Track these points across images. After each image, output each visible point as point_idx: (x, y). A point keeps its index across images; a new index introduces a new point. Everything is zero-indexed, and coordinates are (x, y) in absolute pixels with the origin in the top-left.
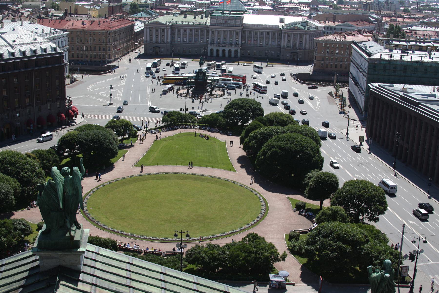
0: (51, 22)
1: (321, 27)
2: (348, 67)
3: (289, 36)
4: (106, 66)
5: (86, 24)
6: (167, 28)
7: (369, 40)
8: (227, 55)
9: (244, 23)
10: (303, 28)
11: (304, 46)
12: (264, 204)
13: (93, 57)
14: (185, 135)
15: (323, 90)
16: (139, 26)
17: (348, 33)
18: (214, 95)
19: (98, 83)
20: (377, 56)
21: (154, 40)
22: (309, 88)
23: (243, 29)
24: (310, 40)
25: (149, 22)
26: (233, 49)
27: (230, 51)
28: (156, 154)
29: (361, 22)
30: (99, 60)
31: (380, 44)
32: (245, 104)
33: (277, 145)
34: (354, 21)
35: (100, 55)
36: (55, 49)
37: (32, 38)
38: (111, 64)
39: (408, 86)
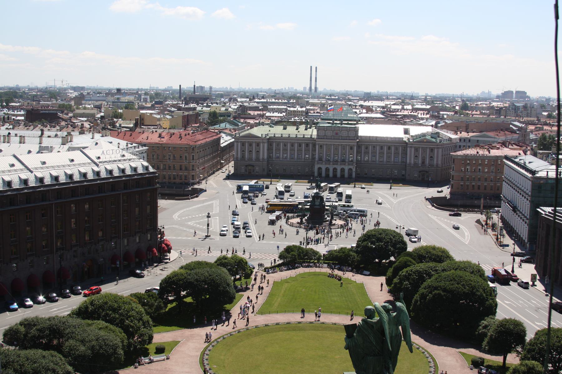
0: (120, 134)
1: (456, 139)
2: (500, 189)
3: (416, 150)
4: (190, 189)
5: (164, 138)
6: (263, 142)
7: (520, 154)
8: (339, 174)
9: (359, 135)
10: (434, 140)
11: (435, 163)
12: (431, 360)
13: (172, 178)
14: (309, 276)
15: (468, 219)
16: (225, 140)
17: (491, 146)
18: (334, 224)
19: (185, 210)
20: (542, 174)
21: (247, 157)
22: (450, 215)
23: (358, 142)
24: (442, 156)
25: (241, 135)
26: (346, 168)
27: (343, 170)
28: (279, 299)
29: (501, 132)
30: (181, 181)
31: (542, 159)
32: (383, 236)
33: (440, 286)
34: (493, 130)
35: (181, 176)
36: (147, 168)
37: (119, 155)
38: (196, 186)
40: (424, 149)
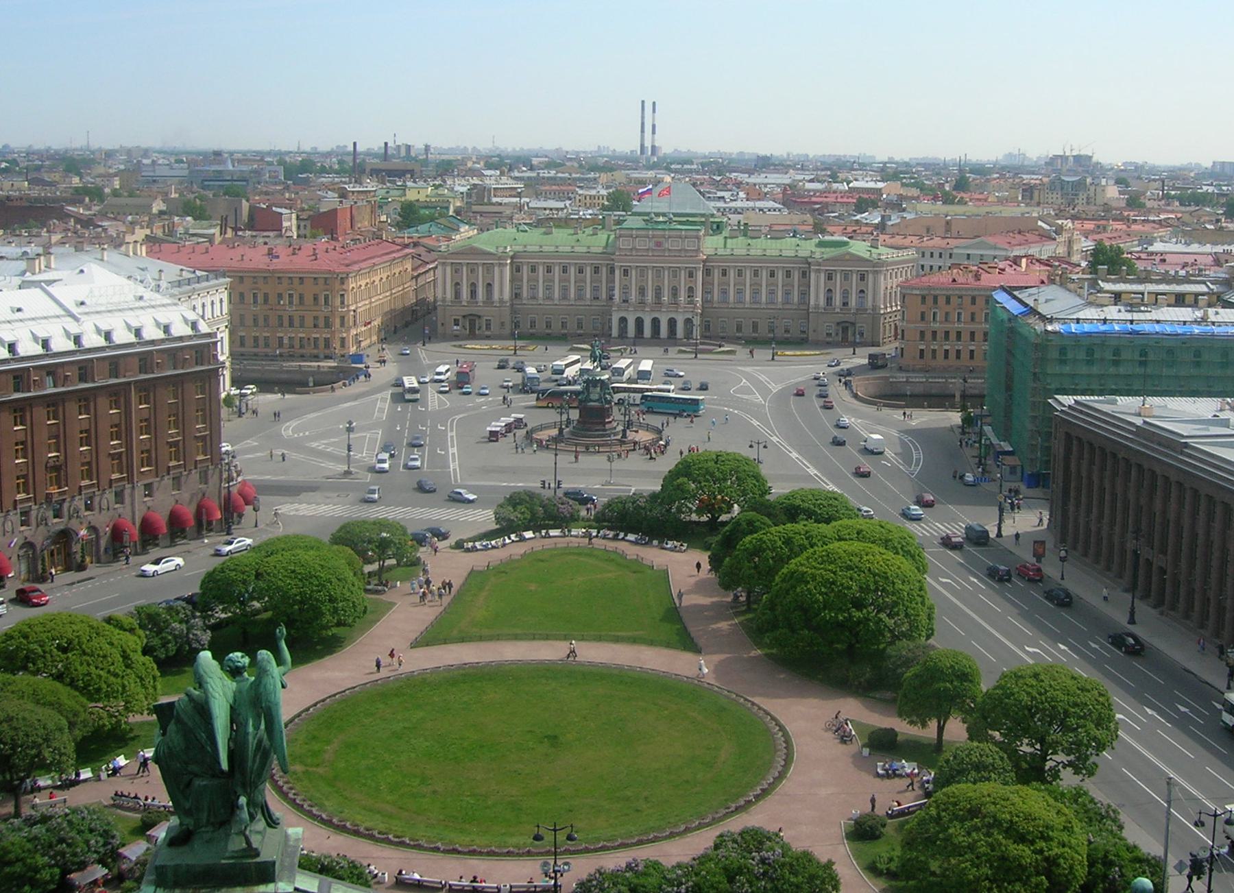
3: (830, 278)
23: (704, 261)
39: (1153, 401)
40: (846, 276)
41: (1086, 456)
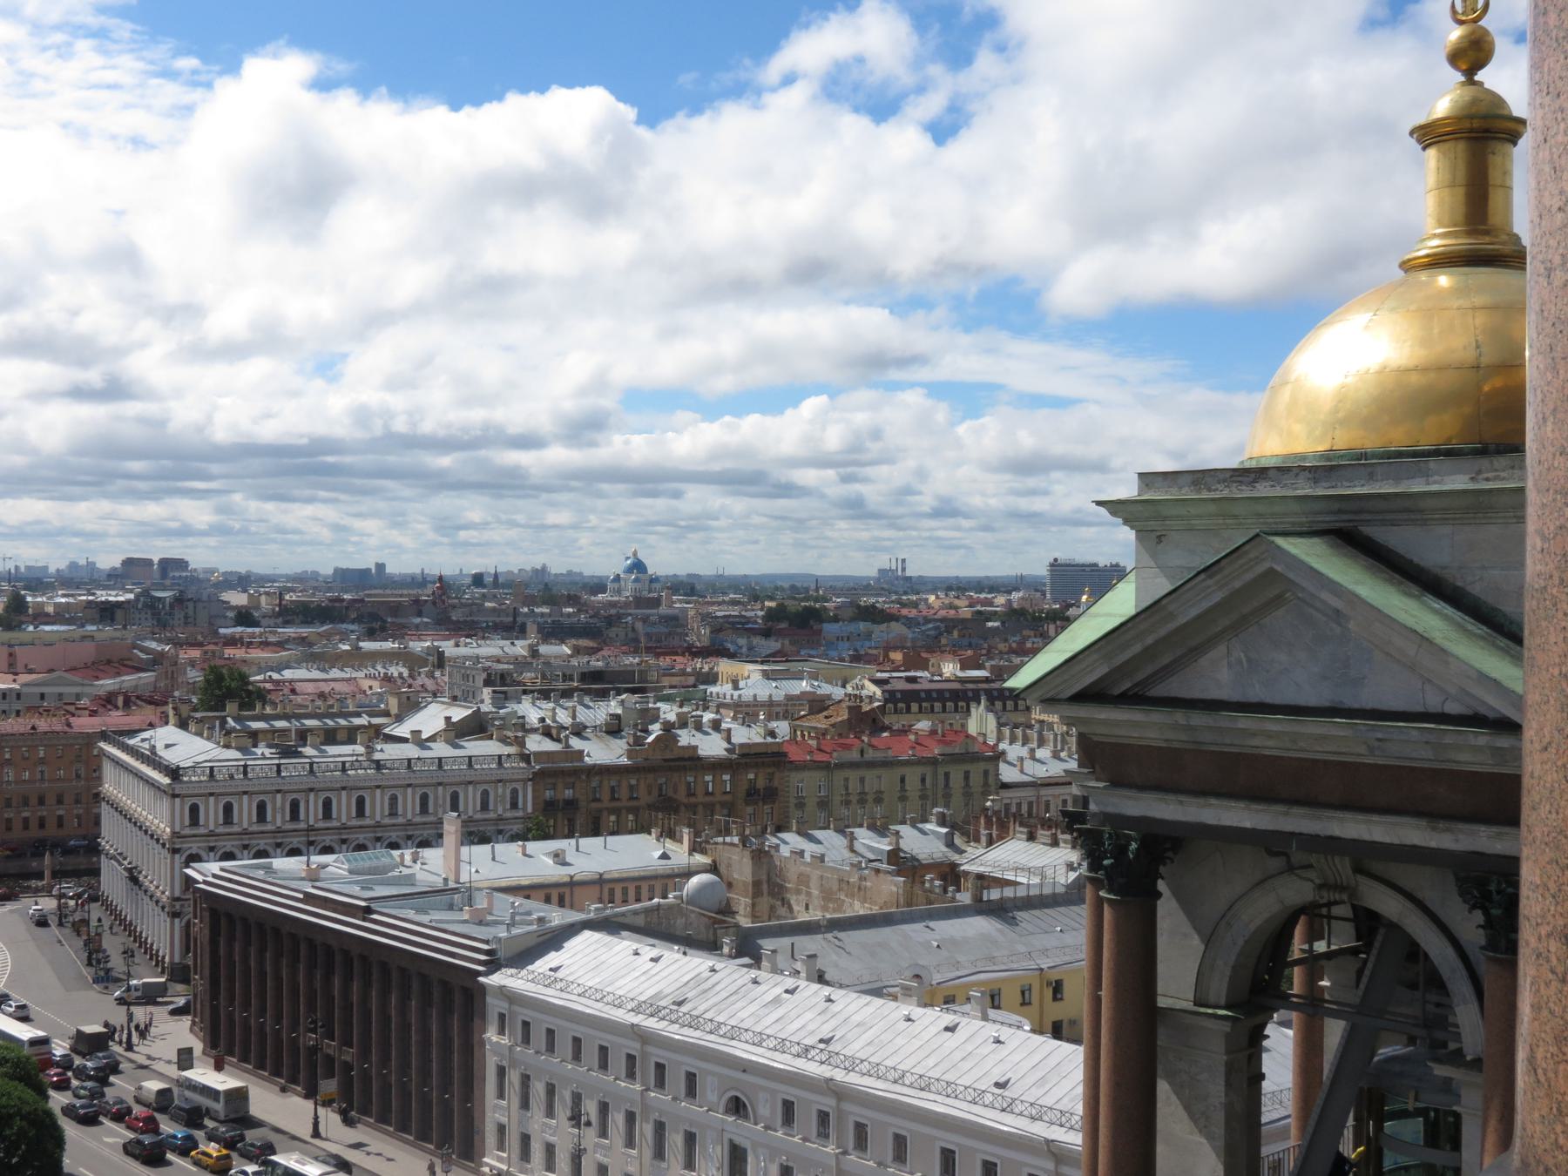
31: (199, 734)
41: (239, 933)
